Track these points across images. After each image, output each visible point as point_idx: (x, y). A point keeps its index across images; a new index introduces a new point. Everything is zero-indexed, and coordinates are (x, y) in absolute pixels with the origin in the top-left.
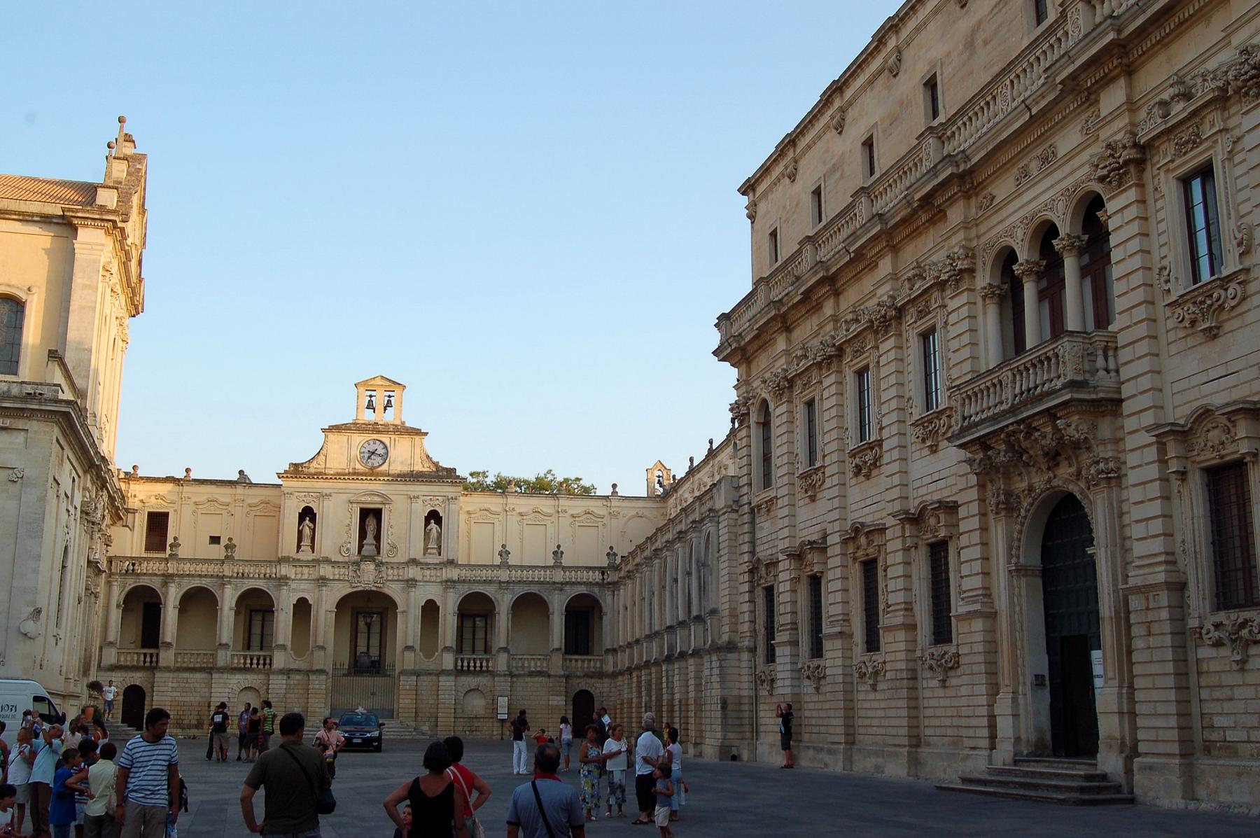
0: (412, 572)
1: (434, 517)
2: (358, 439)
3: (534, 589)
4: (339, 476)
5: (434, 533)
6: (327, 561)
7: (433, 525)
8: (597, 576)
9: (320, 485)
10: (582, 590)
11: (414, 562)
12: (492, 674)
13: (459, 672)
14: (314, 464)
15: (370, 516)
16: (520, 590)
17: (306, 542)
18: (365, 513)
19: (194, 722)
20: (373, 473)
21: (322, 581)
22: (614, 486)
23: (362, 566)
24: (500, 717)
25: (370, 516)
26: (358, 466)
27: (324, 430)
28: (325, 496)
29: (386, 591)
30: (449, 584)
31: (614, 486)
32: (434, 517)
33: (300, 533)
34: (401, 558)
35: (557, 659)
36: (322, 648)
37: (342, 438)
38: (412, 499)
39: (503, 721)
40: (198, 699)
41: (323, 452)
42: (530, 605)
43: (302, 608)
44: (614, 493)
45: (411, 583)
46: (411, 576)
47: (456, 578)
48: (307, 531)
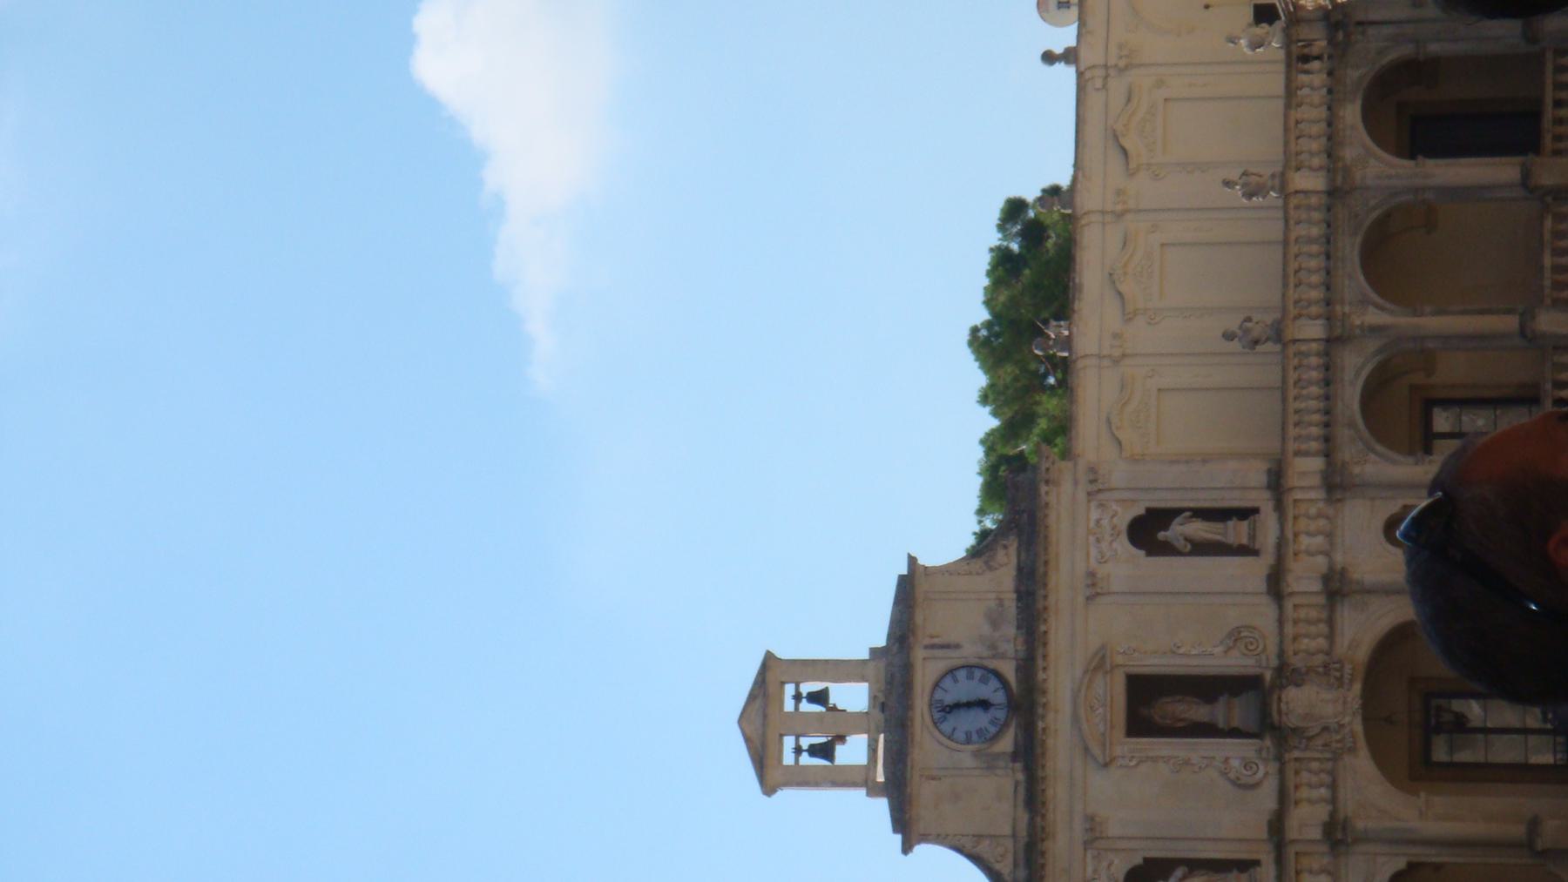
0: (1304, 579)
1: (1148, 531)
2: (928, 747)
3: (1350, 249)
4: (1033, 797)
5: (1200, 530)
6: (1277, 826)
7: (1178, 531)
8: (1314, 78)
10: (1351, 113)
11: (1276, 584)
14: (1005, 868)
15: (1156, 704)
16: (1353, 281)
18: (1139, 724)
20: (1025, 704)
21: (1337, 835)
22: (1049, 58)
23: (1293, 721)
25: (1156, 704)
26: (1006, 744)
27: (907, 848)
28: (1094, 834)
29: (1363, 654)
30: (1336, 485)
31: (1049, 58)
32: (1148, 531)
34: (1264, 615)
35: (1551, 172)
36: (1534, 824)
37: (924, 792)
38: (1094, 589)
41: (968, 843)
42: (1391, 248)
44: (1069, 56)
45: (1336, 588)
46: (1317, 586)
47: (1317, 463)
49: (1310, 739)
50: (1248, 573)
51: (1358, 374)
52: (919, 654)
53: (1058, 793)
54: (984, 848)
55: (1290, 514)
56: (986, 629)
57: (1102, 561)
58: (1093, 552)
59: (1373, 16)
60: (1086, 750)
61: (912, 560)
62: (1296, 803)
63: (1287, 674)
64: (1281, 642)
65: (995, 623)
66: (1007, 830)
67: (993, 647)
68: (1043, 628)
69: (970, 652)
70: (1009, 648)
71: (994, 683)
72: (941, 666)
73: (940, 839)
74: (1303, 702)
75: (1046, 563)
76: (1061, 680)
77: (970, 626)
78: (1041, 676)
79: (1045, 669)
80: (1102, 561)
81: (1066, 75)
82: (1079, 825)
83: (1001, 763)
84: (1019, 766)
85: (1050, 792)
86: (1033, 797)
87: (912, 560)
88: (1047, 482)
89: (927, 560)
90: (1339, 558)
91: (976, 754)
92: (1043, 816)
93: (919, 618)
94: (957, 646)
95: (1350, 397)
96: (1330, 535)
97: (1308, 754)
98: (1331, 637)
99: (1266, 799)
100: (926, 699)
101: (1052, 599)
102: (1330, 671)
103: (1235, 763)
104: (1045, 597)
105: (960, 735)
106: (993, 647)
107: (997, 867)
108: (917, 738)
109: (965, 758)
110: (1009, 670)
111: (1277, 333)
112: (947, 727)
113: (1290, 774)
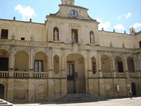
1: (91, 33)
6: (63, 43)
9: (59, 20)
11: (88, 45)
12: (114, 78)
13: (104, 78)
14: (57, 15)
15: (75, 32)
17: (56, 38)
19: (23, 97)
24: (118, 91)
25: (75, 32)
26: (70, 16)
28: (62, 24)
32: (91, 33)
33: (54, 35)
34: (85, 43)
37: (65, 8)
39: (118, 92)
40: (23, 89)
43: (56, 59)
45: (88, 51)
47: (100, 50)
48: (56, 35)
49: (72, 47)
50: (88, 42)
51: (108, 54)
52: (79, 9)
53: (65, 20)
54: (59, 13)
55: (95, 47)
56: (82, 16)
57: (89, 28)
58: (90, 27)
59: (138, 57)
60: (70, 24)
61: (88, 9)
62: (65, 45)
63: (79, 45)
64: (81, 45)
65: (82, 17)
66: (61, 15)
67: (80, 16)
68: (82, 21)
69: (79, 14)
70: (80, 18)
71: (76, 16)
72: (78, 12)
73: (60, 9)
74: (76, 47)
75: (89, 22)
76: (77, 22)
77: (82, 14)
78: (78, 20)
79: (78, 21)
80: (89, 28)
81: (124, 33)
82: (62, 22)
83: (68, 15)
84: (68, 17)
85: (66, 20)
86: (65, 18)
87: (88, 9)
88: (96, 23)
89: (88, 11)
90: (91, 51)
91: (69, 13)
92: (63, 19)
93: (82, 9)
94: (80, 13)
95: (106, 54)
96: (93, 50)
97: (71, 47)
98: (82, 50)
99: (65, 42)
100: (74, 9)
101: (85, 22)
102: (80, 50)
103: (69, 39)
104: (85, 21)
105: (71, 12)
106: (80, 16)
107: (58, 14)
108: (71, 8)
109: (69, 12)
110: (77, 18)
111: (111, 46)
112: (72, 11)
113: (68, 45)
